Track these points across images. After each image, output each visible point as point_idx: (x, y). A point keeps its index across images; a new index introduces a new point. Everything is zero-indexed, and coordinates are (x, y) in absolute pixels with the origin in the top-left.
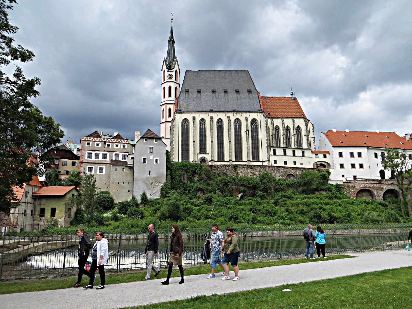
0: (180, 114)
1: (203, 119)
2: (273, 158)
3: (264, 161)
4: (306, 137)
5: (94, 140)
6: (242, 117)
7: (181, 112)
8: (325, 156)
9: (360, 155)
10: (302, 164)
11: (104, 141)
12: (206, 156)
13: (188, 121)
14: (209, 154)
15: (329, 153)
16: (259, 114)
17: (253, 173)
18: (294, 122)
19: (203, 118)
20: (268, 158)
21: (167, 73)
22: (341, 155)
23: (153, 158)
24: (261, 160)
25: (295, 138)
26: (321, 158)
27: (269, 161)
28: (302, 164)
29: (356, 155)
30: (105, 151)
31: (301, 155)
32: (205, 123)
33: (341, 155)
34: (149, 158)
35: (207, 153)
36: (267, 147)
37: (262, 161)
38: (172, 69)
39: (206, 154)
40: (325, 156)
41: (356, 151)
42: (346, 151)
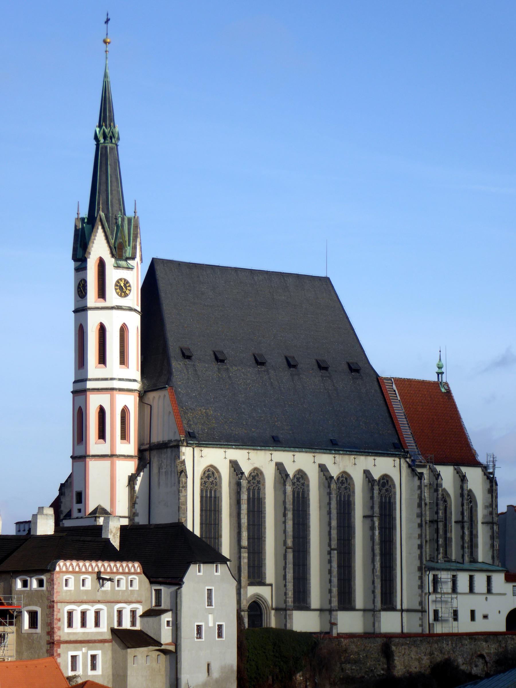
0: (197, 450)
1: (256, 469)
3: (408, 611)
4: (487, 528)
5: (77, 569)
6: (357, 467)
10: (485, 617)
11: (96, 570)
12: (265, 592)
13: (216, 475)
14: (271, 585)
16: (397, 460)
17: (419, 660)
18: (463, 478)
19: (257, 465)
20: (421, 603)
21: (113, 275)
23: (214, 623)
24: (399, 607)
25: (467, 532)
28: (485, 617)
30: (99, 602)
31: (485, 590)
32: (259, 482)
34: (207, 623)
35: (268, 581)
36: (420, 569)
37: (402, 611)
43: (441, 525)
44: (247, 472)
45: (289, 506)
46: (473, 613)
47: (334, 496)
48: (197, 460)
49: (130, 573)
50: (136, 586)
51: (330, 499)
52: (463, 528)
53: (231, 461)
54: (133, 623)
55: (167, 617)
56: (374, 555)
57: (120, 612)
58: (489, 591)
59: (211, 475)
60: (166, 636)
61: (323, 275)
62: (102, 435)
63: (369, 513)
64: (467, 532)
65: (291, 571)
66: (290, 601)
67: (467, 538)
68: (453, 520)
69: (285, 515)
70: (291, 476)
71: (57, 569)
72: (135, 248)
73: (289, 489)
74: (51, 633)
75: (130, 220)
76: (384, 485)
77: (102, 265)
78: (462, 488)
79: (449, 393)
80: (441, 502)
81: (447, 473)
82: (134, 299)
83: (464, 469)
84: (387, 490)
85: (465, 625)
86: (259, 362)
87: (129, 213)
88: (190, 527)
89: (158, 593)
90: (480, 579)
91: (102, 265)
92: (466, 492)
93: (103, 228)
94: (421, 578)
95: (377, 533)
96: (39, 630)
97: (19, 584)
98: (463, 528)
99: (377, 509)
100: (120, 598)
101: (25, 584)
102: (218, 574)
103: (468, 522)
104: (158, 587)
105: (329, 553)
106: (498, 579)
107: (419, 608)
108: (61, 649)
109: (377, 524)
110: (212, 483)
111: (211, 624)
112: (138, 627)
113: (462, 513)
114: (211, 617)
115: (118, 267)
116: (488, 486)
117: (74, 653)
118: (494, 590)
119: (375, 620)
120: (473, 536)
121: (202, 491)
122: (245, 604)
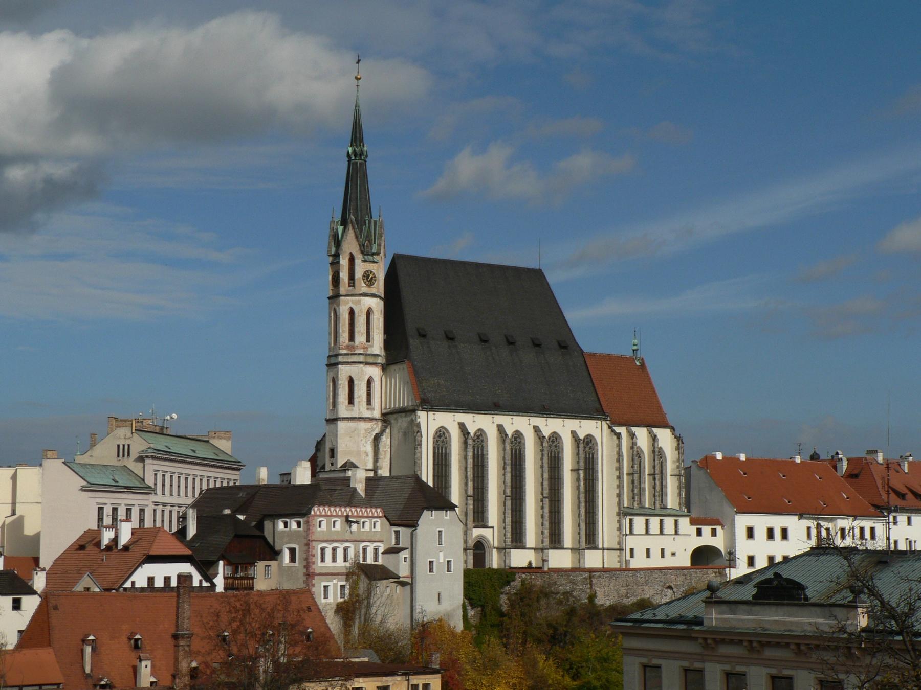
0: (431, 413)
1: (480, 430)
2: (630, 542)
3: (608, 549)
4: (676, 478)
6: (565, 428)
7: (434, 409)
8: (714, 533)
9: (785, 534)
10: (673, 554)
12: (486, 533)
13: (447, 435)
14: (492, 527)
15: (723, 526)
16: (599, 422)
18: (654, 438)
20: (619, 543)
21: (360, 268)
22: (750, 533)
24: (601, 546)
25: (658, 483)
26: (707, 539)
27: (621, 550)
28: (673, 554)
29: (778, 534)
30: (347, 541)
32: (482, 441)
33: (750, 533)
34: (438, 559)
36: (618, 514)
37: (603, 549)
38: (373, 254)
39: (486, 527)
40: (714, 533)
41: (778, 522)
42: (760, 522)
43: (636, 476)
44: (472, 433)
45: (508, 461)
46: (663, 550)
47: (546, 452)
48: (431, 422)
49: (373, 517)
50: (378, 528)
51: (542, 455)
52: (654, 479)
53: (459, 423)
54: (376, 559)
55: (405, 554)
56: (579, 502)
57: (365, 550)
58: (676, 533)
59: (442, 436)
60: (403, 571)
61: (536, 267)
62: (351, 401)
63: (576, 467)
64: (658, 483)
65: (510, 516)
66: (509, 540)
67: (658, 488)
68: (647, 473)
69: (504, 469)
70: (510, 436)
71: (312, 513)
72: (379, 245)
73: (508, 447)
74: (307, 567)
75: (375, 222)
76: (588, 443)
77: (352, 259)
78: (653, 445)
79: (643, 365)
80: (636, 458)
81: (642, 434)
82: (379, 287)
83: (655, 430)
84: (590, 448)
85: (656, 562)
86: (484, 341)
87: (375, 218)
88: (424, 479)
89: (397, 533)
90: (669, 522)
91: (352, 259)
92: (657, 450)
93: (353, 228)
94: (619, 522)
95: (582, 483)
96: (297, 564)
97: (281, 526)
98: (654, 479)
99: (582, 464)
100: (364, 538)
101: (286, 526)
102: (448, 517)
103: (658, 474)
104: (397, 529)
105: (542, 501)
106: (684, 522)
107: (618, 547)
108: (316, 580)
109: (582, 476)
110: (443, 441)
111: (441, 561)
112: (380, 562)
113: (654, 467)
114: (441, 554)
115: (365, 261)
116: (676, 445)
117: (327, 584)
118: (681, 531)
119: (580, 558)
120: (663, 487)
121: (434, 448)
122: (471, 543)
